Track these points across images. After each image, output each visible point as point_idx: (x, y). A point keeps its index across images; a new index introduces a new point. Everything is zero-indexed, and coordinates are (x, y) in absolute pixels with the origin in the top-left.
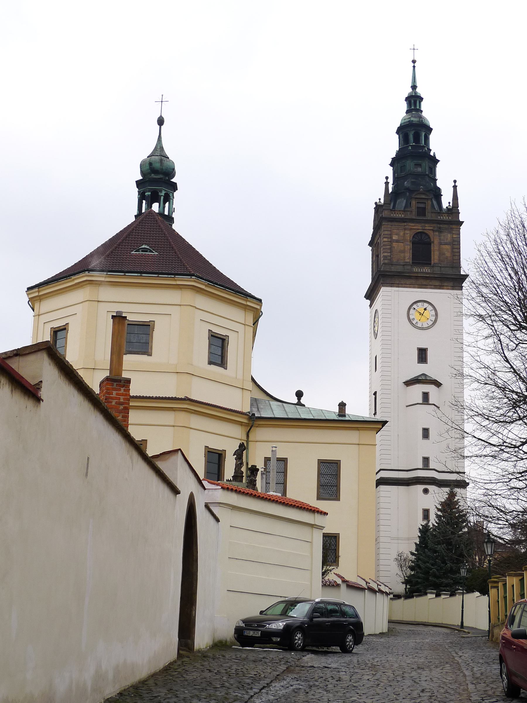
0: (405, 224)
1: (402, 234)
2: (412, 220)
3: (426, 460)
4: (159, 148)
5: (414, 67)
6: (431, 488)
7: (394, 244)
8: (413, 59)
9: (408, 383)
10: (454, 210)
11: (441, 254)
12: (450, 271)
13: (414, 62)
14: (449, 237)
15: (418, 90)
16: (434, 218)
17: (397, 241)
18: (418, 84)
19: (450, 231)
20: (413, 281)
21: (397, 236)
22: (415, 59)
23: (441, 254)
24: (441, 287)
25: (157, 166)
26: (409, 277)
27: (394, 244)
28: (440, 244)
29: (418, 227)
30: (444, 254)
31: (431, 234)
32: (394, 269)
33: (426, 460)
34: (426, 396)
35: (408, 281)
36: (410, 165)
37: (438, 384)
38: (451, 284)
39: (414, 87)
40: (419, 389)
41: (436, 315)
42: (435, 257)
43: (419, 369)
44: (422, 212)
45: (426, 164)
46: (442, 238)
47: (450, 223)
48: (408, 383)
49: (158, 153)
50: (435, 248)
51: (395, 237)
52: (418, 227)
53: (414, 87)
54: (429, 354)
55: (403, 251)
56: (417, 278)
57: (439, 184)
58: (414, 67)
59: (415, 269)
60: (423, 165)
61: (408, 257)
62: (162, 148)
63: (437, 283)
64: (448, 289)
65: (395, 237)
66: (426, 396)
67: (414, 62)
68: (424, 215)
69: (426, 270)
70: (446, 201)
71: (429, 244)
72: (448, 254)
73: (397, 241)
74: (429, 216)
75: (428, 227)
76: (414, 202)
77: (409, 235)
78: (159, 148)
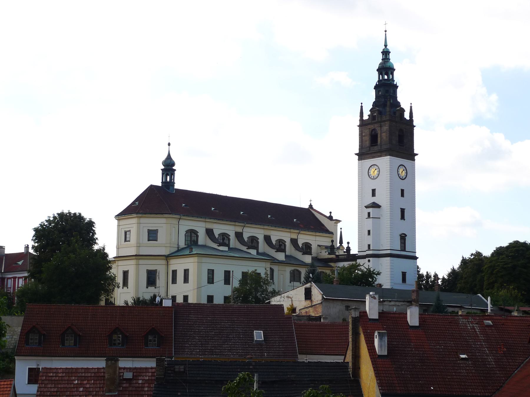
0: (367, 126)
3: (369, 246)
4: (169, 155)
5: (386, 34)
6: (371, 259)
8: (385, 30)
9: (367, 207)
13: (386, 31)
15: (387, 47)
17: (364, 136)
21: (364, 133)
22: (386, 30)
28: (381, 133)
29: (372, 127)
30: (383, 138)
33: (369, 246)
34: (369, 214)
35: (368, 156)
38: (385, 153)
39: (386, 46)
46: (382, 130)
48: (367, 207)
50: (379, 136)
52: (372, 127)
53: (386, 46)
54: (376, 191)
55: (366, 141)
58: (386, 34)
61: (368, 143)
63: (379, 154)
64: (384, 156)
66: (369, 214)
67: (386, 31)
68: (375, 119)
69: (376, 148)
73: (364, 136)
75: (376, 126)
78: (169, 155)
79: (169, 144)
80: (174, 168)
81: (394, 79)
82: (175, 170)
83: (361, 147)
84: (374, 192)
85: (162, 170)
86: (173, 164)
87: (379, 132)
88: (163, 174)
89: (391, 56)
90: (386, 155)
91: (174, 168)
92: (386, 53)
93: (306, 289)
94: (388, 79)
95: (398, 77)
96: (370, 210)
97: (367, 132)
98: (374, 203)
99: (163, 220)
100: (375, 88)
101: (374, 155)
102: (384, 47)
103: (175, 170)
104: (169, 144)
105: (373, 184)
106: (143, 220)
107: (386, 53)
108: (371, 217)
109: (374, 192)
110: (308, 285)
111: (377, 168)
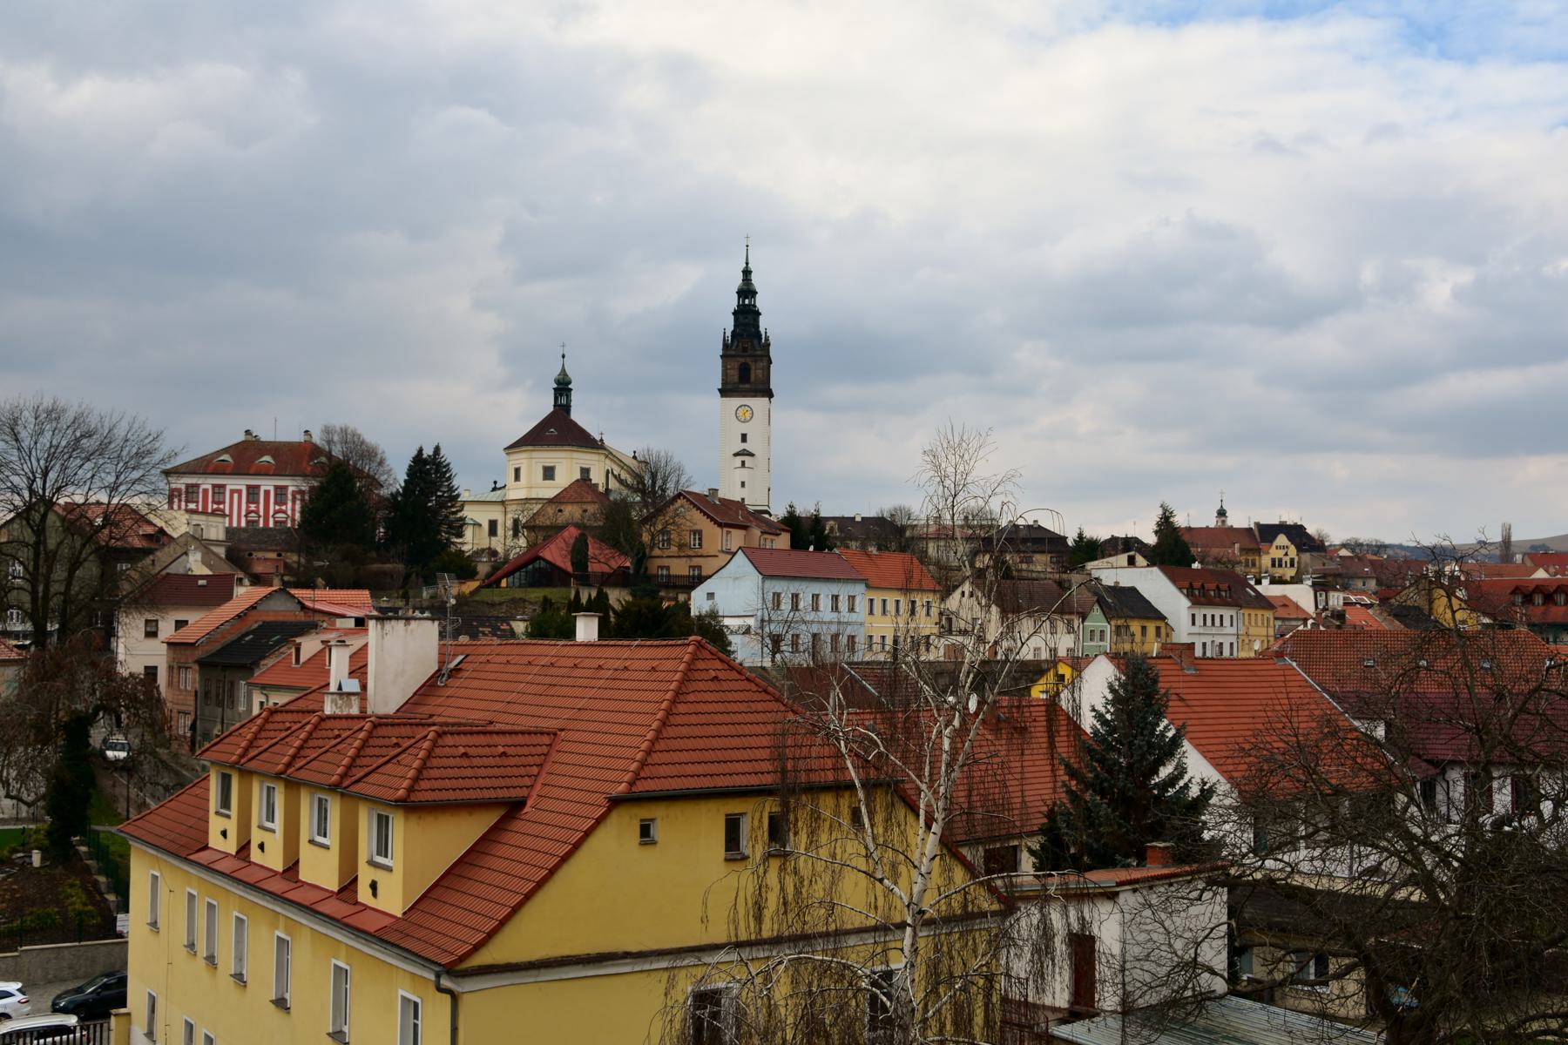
2: (739, 356)
4: (563, 370)
9: (736, 455)
11: (756, 375)
18: (750, 261)
23: (756, 375)
24: (755, 396)
29: (743, 360)
32: (729, 387)
34: (743, 463)
36: (741, 318)
37: (752, 455)
39: (747, 264)
40: (740, 459)
43: (741, 446)
44: (745, 350)
48: (736, 455)
50: (752, 372)
52: (743, 360)
53: (747, 264)
54: (748, 438)
56: (741, 392)
59: (741, 386)
61: (736, 378)
66: (743, 463)
69: (747, 386)
71: (749, 370)
74: (750, 352)
75: (748, 359)
78: (563, 370)
79: (563, 356)
82: (571, 390)
83: (724, 382)
84: (744, 438)
86: (570, 383)
87: (753, 368)
88: (555, 394)
89: (753, 277)
90: (763, 396)
92: (747, 273)
93: (1129, 556)
94: (749, 305)
95: (761, 302)
96: (746, 458)
97: (734, 364)
99: (595, 457)
100: (735, 313)
103: (571, 390)
104: (563, 356)
105: (744, 429)
106: (576, 455)
107: (747, 273)
109: (744, 438)
110: (1132, 553)
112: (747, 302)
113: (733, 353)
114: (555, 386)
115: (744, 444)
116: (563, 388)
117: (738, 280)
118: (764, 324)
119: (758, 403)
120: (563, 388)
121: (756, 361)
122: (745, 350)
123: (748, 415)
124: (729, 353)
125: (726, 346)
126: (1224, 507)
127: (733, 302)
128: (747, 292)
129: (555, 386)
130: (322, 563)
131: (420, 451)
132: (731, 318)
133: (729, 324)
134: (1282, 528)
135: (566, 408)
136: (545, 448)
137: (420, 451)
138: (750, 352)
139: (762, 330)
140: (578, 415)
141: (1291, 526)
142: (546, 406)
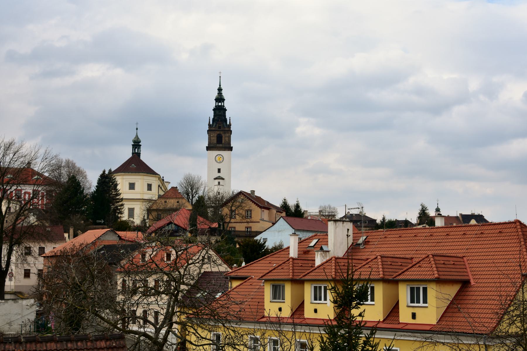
1: (214, 134)
4: (137, 136)
7: (211, 138)
9: (215, 179)
10: (230, 125)
11: (225, 140)
12: (228, 146)
13: (220, 77)
14: (227, 135)
15: (221, 86)
16: (223, 129)
17: (212, 137)
18: (221, 84)
19: (228, 133)
20: (217, 149)
23: (225, 140)
24: (225, 150)
25: (136, 141)
26: (216, 148)
27: (211, 138)
29: (219, 132)
31: (222, 134)
32: (211, 146)
34: (219, 183)
36: (217, 112)
37: (223, 179)
39: (220, 85)
40: (217, 181)
41: (223, 159)
42: (223, 142)
43: (219, 175)
44: (220, 127)
45: (222, 112)
47: (228, 131)
48: (215, 179)
49: (137, 137)
50: (223, 138)
51: (212, 136)
52: (219, 132)
53: (220, 85)
54: (221, 170)
55: (214, 140)
56: (218, 148)
57: (226, 117)
59: (218, 145)
60: (221, 112)
61: (215, 141)
62: (137, 136)
63: (224, 149)
65: (212, 136)
66: (219, 183)
67: (220, 77)
69: (221, 145)
70: (228, 123)
71: (222, 137)
72: (227, 140)
73: (212, 137)
74: (222, 129)
75: (221, 132)
76: (217, 125)
77: (216, 135)
78: (137, 136)
79: (137, 129)
80: (140, 144)
81: (225, 105)
82: (141, 145)
84: (219, 171)
85: (132, 145)
86: (140, 142)
87: (224, 136)
88: (133, 148)
91: (140, 144)
92: (220, 90)
94: (221, 106)
97: (214, 135)
98: (219, 176)
99: (154, 179)
101: (220, 149)
102: (219, 86)
103: (141, 145)
104: (137, 129)
107: (220, 90)
108: (220, 184)
109: (219, 171)
111: (222, 157)
112: (220, 104)
113: (214, 129)
114: (133, 144)
115: (219, 174)
116: (137, 144)
117: (215, 94)
118: (228, 115)
119: (225, 153)
120: (137, 144)
121: (225, 133)
122: (220, 127)
123: (221, 159)
124: (212, 129)
125: (209, 125)
126: (439, 207)
127: (213, 104)
128: (220, 99)
129: (133, 144)
130: (101, 221)
131: (104, 172)
132: (212, 113)
133: (211, 114)
134: (473, 216)
135: (139, 154)
136: (130, 174)
137: (104, 172)
138: (222, 129)
139: (227, 117)
140: (145, 157)
141: (476, 215)
142: (127, 154)
